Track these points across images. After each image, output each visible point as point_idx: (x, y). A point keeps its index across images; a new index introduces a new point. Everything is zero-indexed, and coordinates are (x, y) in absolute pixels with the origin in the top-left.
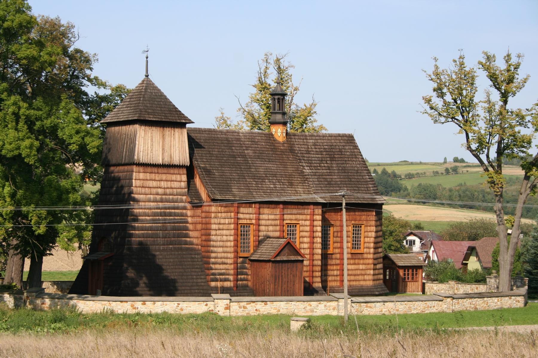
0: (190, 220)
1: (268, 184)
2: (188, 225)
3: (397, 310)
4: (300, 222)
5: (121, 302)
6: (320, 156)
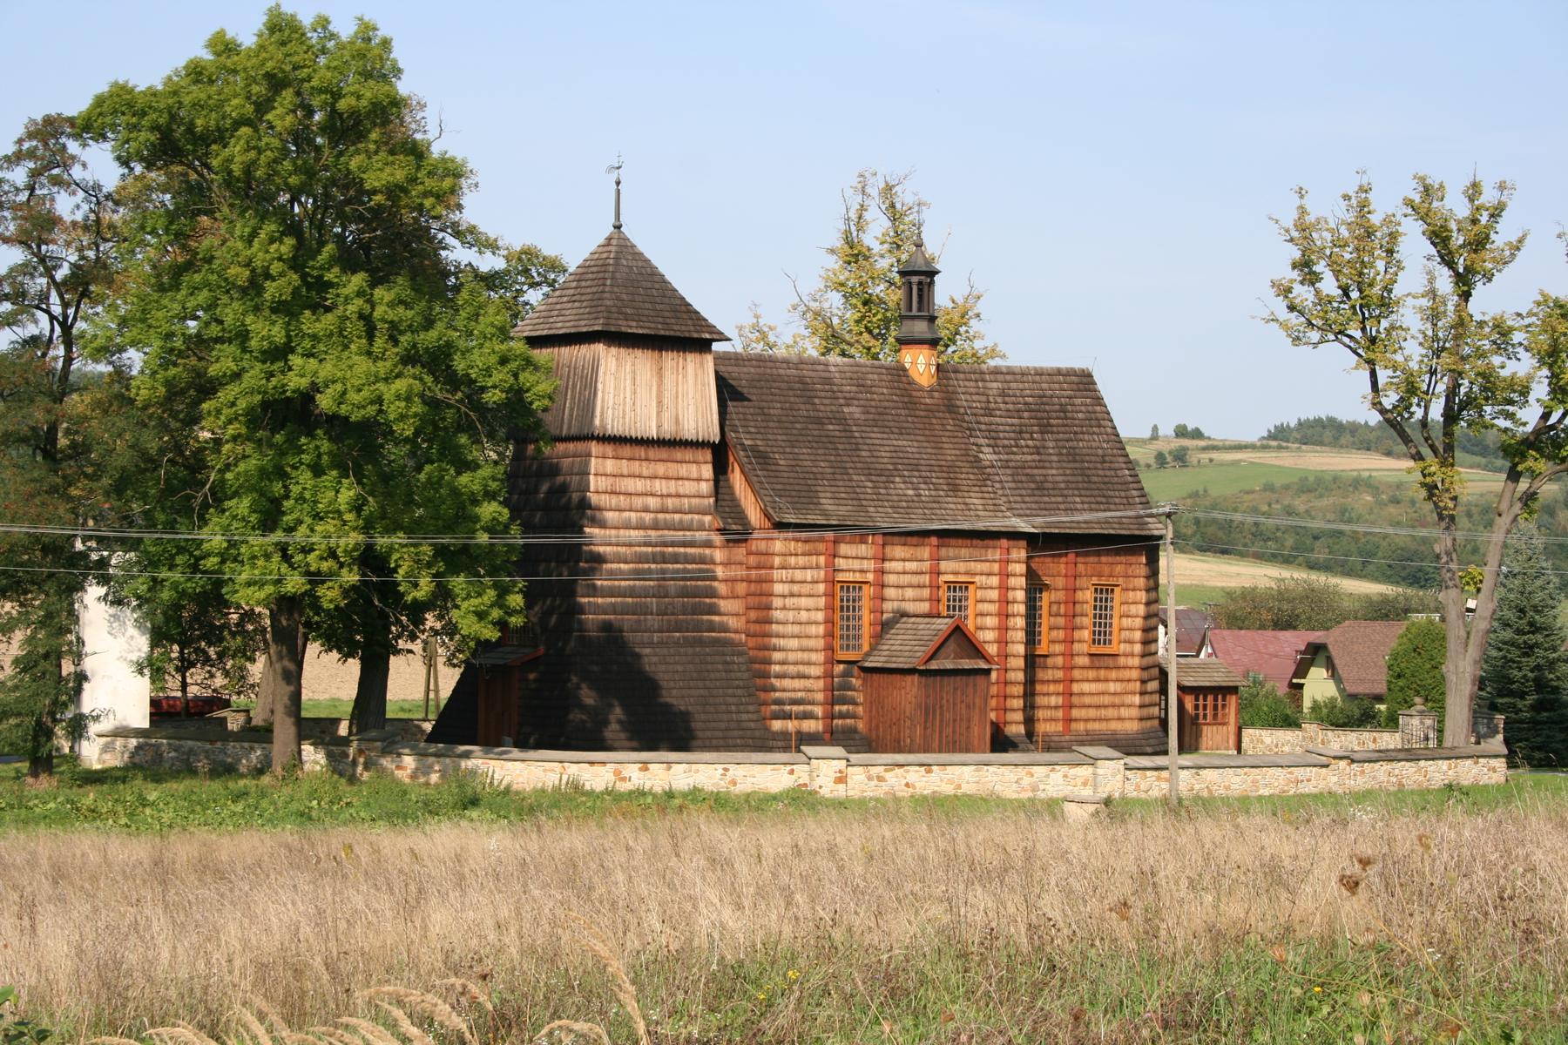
0: (720, 572)
1: (903, 490)
2: (716, 584)
3: (1227, 788)
4: (977, 579)
5: (592, 763)
6: (1015, 421)
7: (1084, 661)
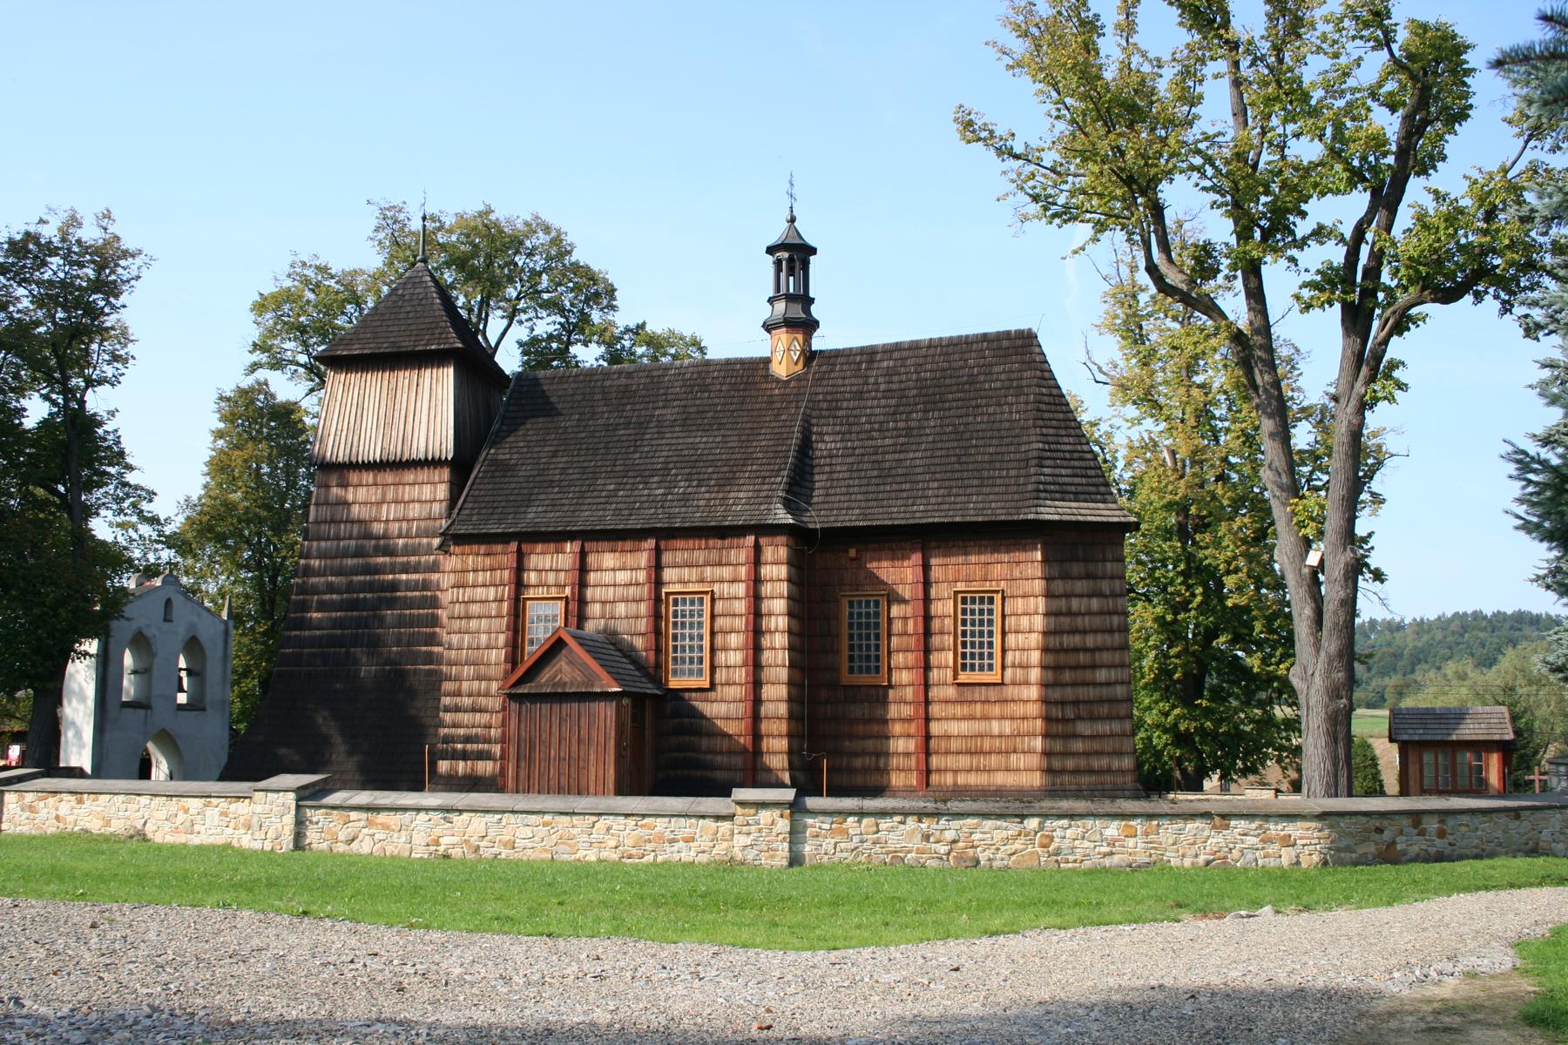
4: (716, 588)
7: (951, 692)
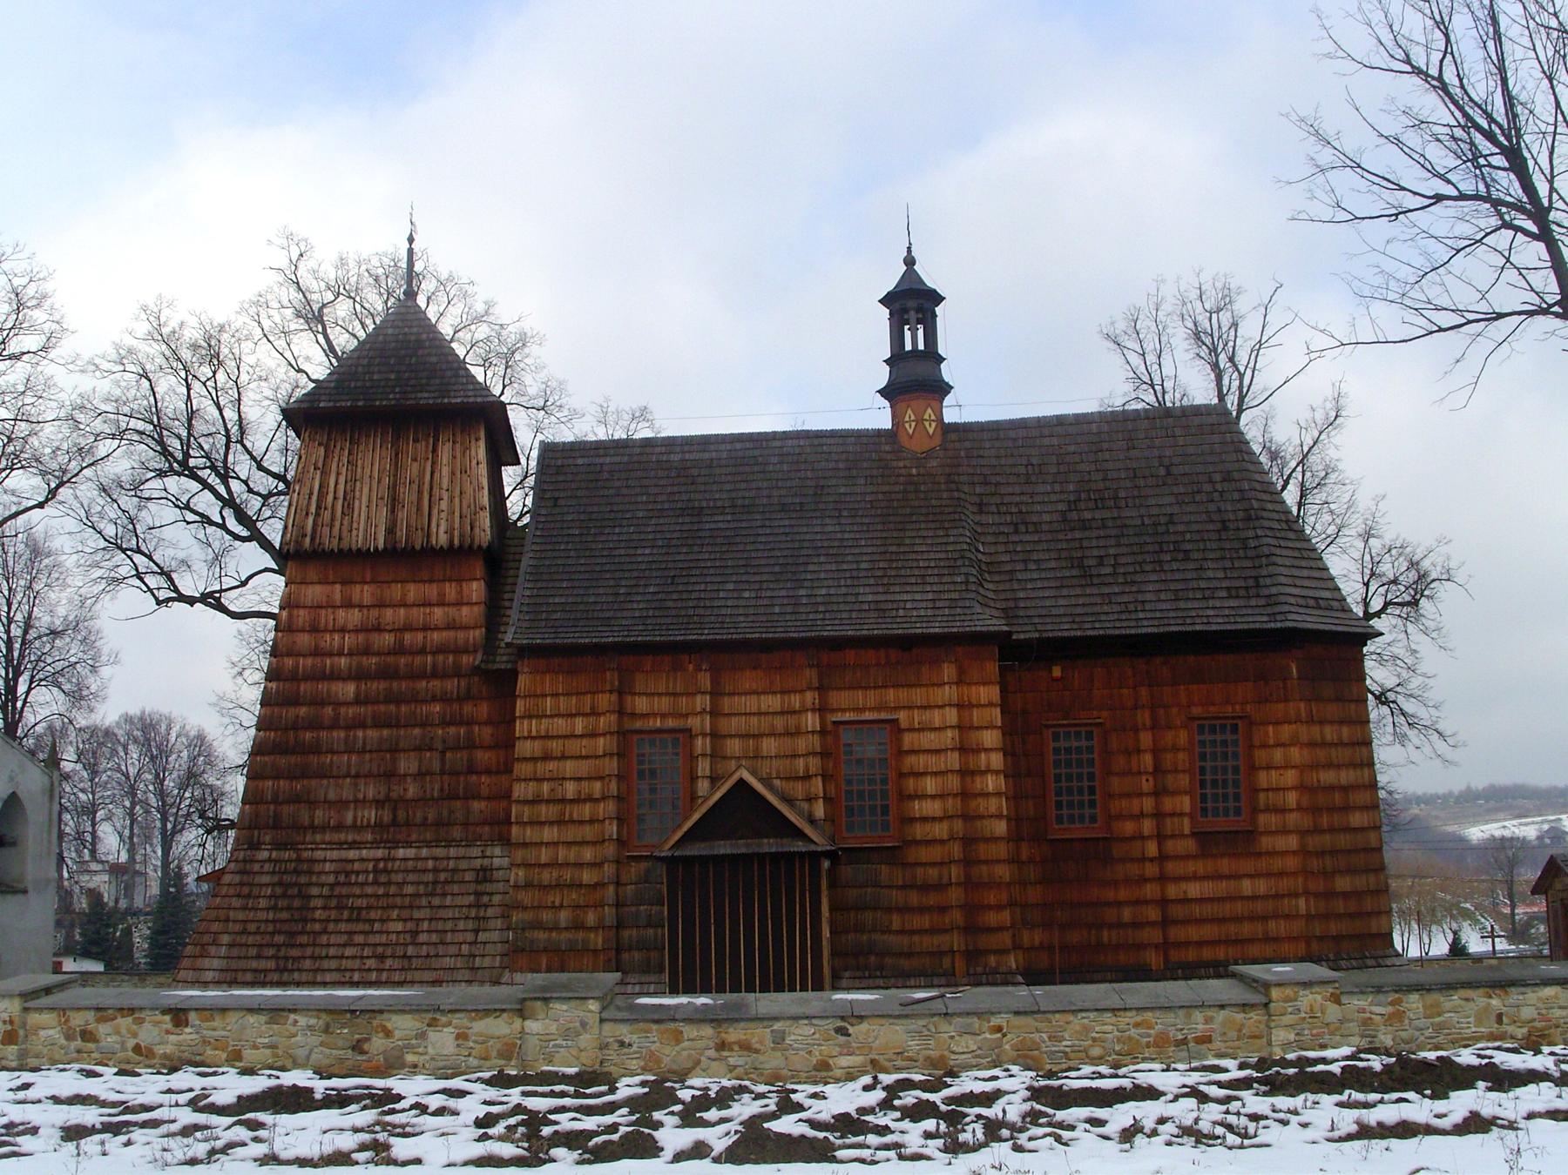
4: (902, 716)
